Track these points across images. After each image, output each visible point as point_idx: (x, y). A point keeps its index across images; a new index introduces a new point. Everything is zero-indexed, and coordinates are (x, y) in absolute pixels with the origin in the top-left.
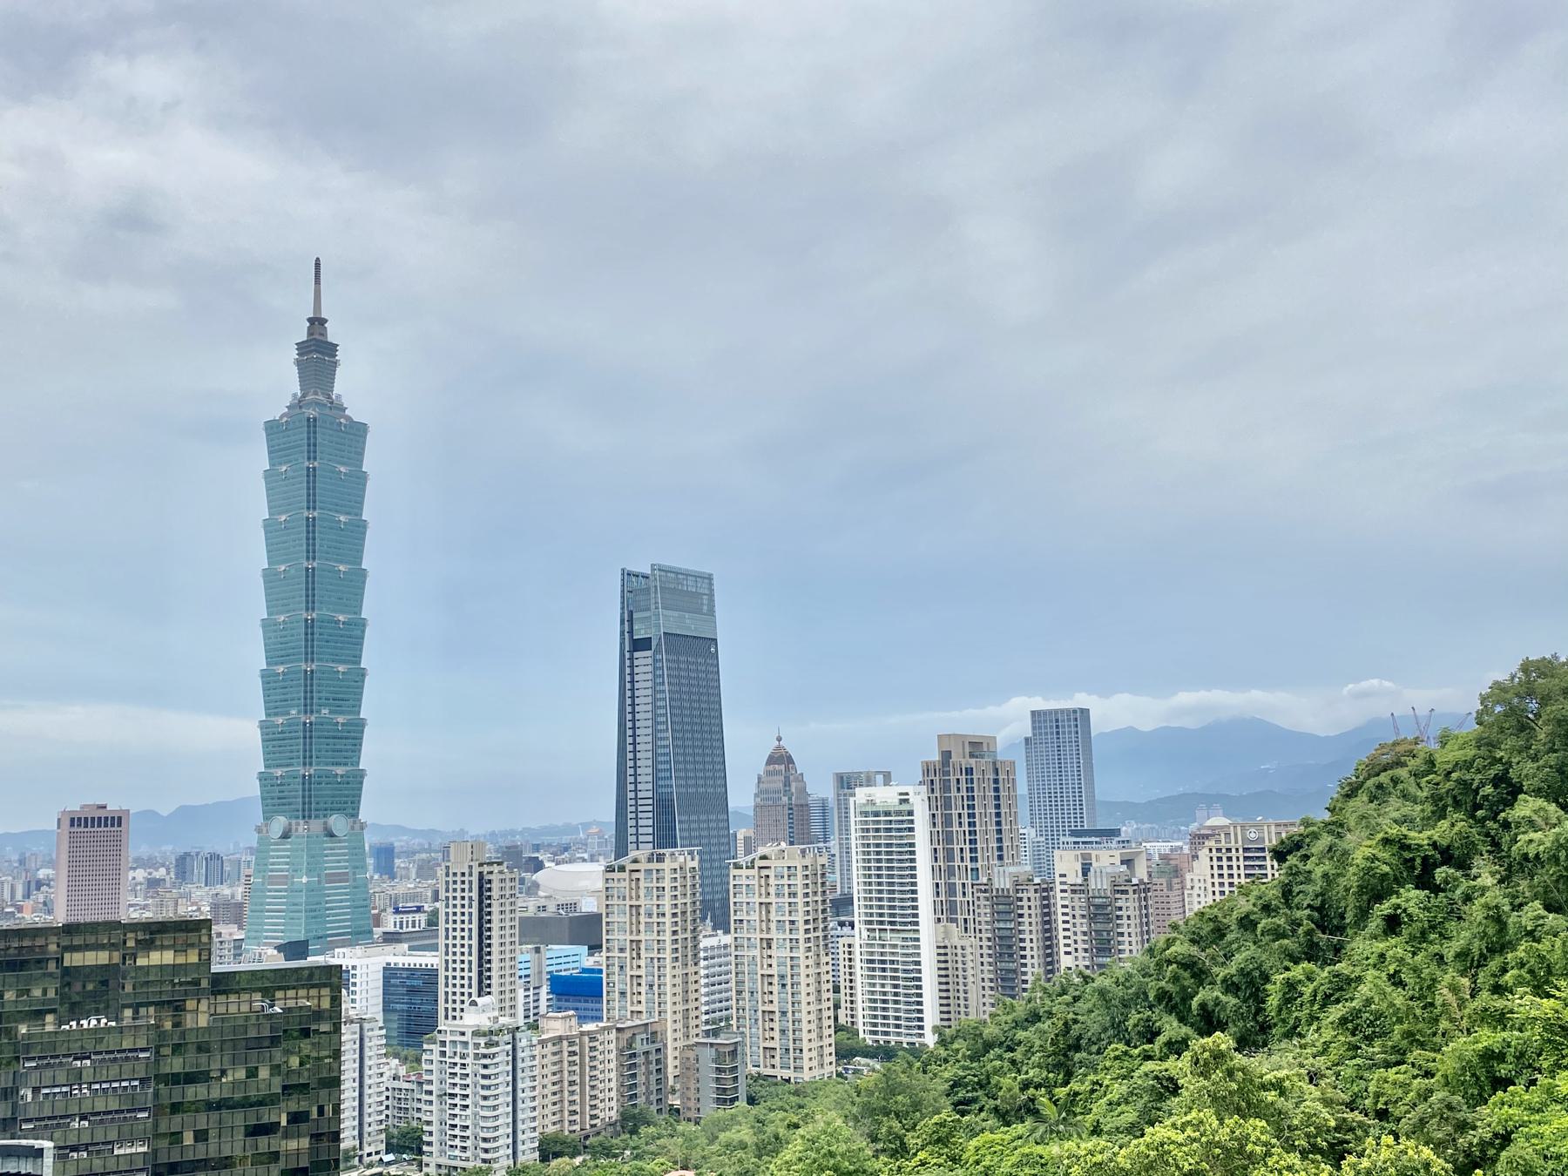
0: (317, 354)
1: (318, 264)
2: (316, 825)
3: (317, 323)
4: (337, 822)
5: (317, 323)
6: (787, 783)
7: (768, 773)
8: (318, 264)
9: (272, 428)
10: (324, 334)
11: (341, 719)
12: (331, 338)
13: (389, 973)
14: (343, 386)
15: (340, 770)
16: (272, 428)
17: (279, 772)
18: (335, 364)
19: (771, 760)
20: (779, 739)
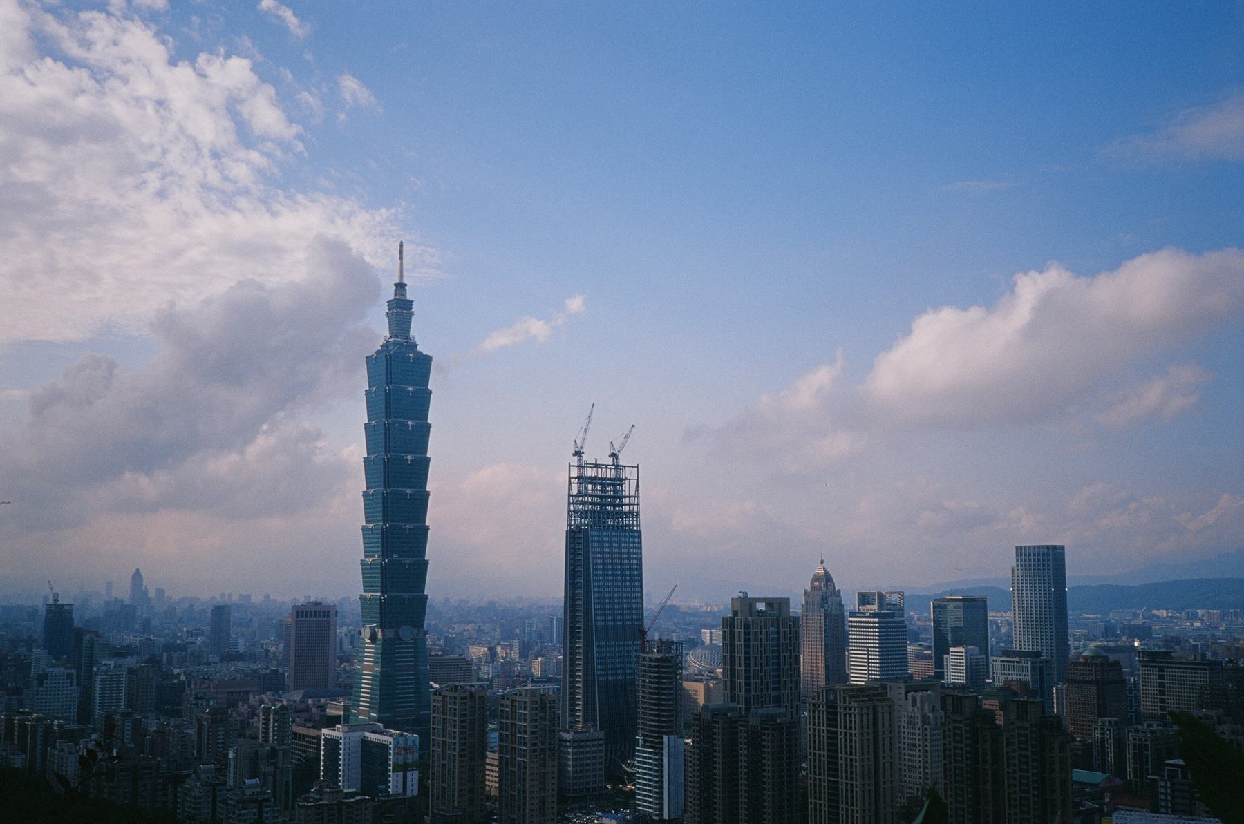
0: (401, 309)
1: (401, 246)
2: (390, 634)
3: (401, 287)
4: (406, 632)
5: (401, 287)
6: (824, 600)
7: (813, 588)
8: (401, 246)
9: (369, 359)
10: (404, 294)
11: (409, 561)
12: (409, 297)
13: (365, 743)
14: (414, 332)
15: (407, 596)
16: (369, 359)
17: (369, 595)
18: (411, 314)
19: (816, 578)
20: (822, 562)
